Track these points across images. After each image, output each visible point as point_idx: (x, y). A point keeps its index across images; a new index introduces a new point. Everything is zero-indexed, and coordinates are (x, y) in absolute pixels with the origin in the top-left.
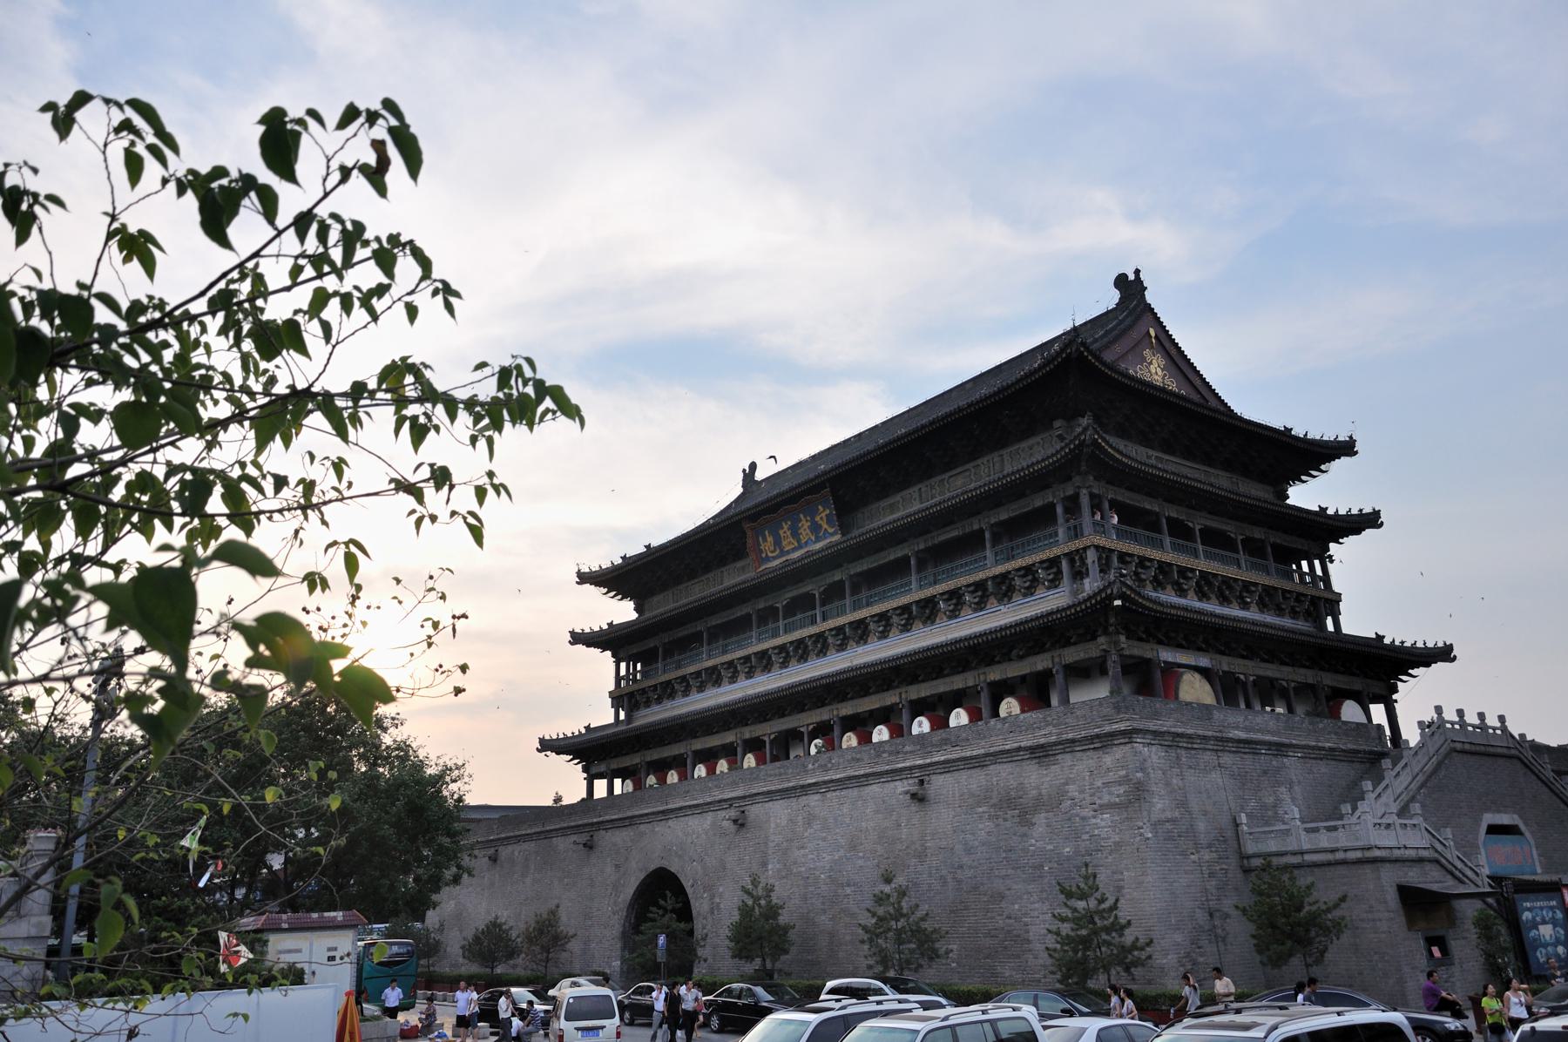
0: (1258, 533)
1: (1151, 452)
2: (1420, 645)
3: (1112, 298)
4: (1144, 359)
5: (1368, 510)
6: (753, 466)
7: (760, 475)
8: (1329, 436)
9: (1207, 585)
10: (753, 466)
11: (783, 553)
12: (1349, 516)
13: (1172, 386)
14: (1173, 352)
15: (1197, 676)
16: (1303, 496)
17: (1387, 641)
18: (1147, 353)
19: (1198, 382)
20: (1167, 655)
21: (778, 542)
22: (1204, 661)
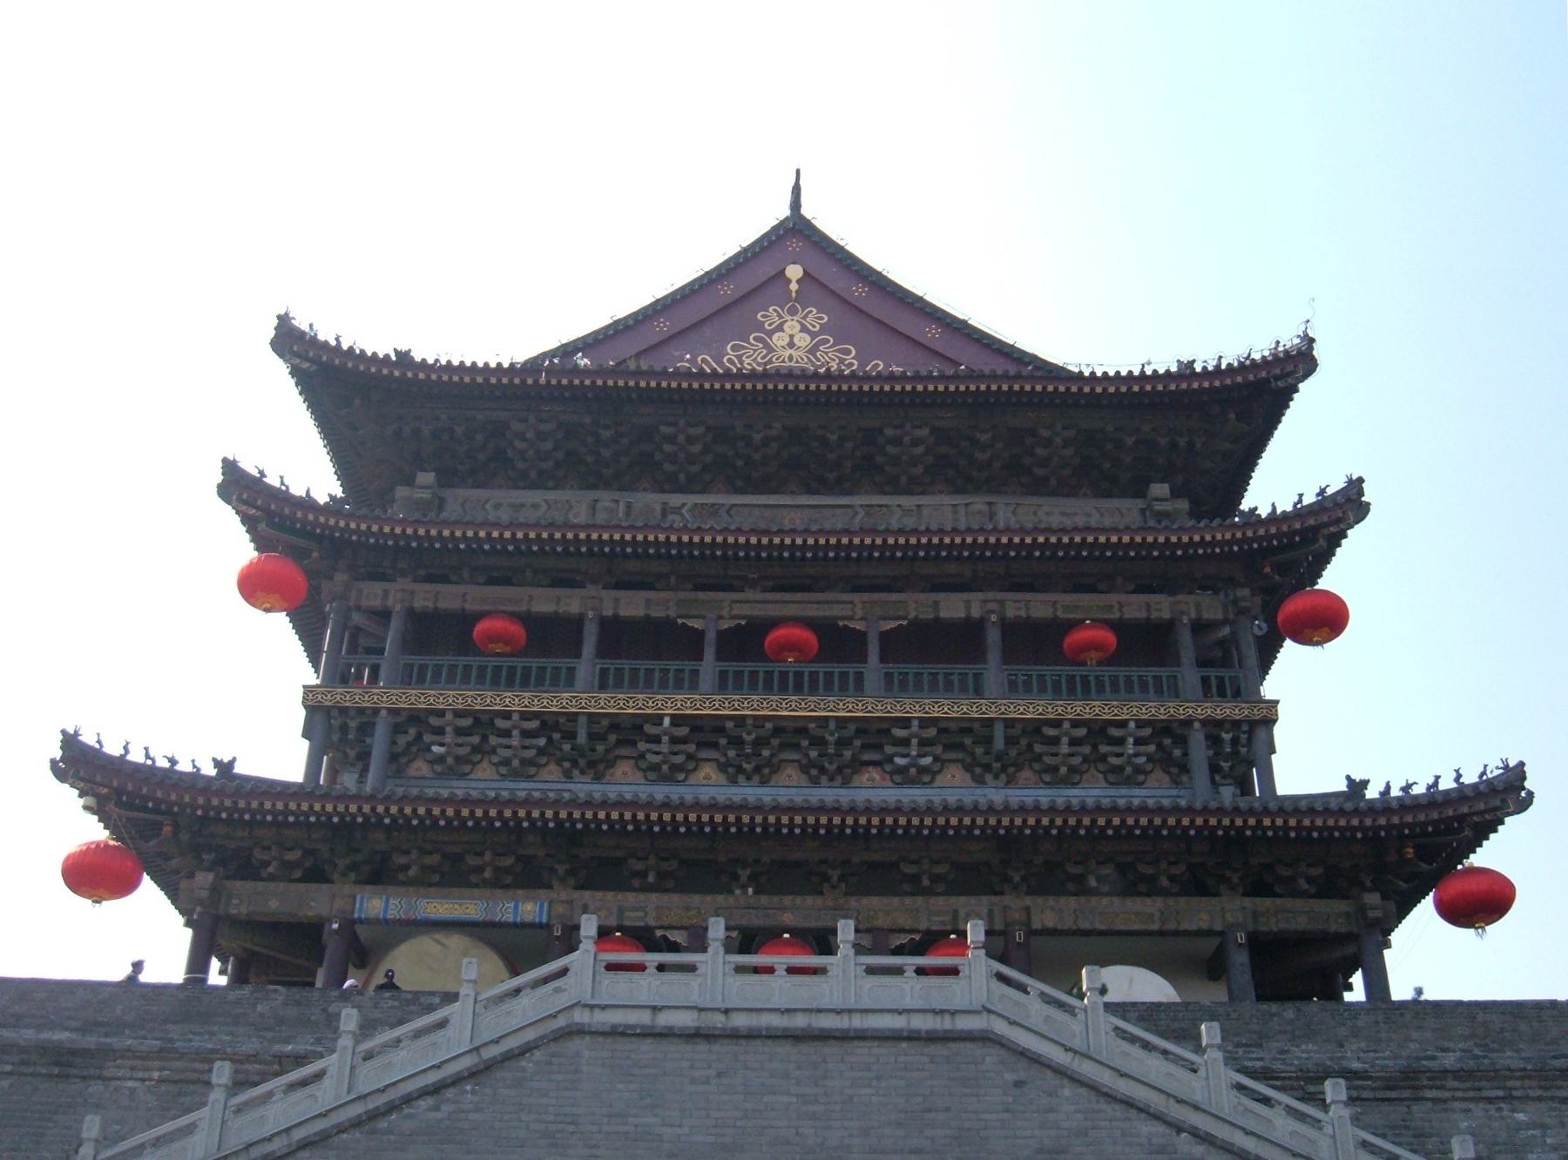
0: (953, 607)
1: (676, 499)
2: (1447, 784)
4: (760, 327)
5: (1336, 485)
8: (1260, 349)
13: (840, 359)
14: (858, 292)
15: (456, 941)
18: (771, 315)
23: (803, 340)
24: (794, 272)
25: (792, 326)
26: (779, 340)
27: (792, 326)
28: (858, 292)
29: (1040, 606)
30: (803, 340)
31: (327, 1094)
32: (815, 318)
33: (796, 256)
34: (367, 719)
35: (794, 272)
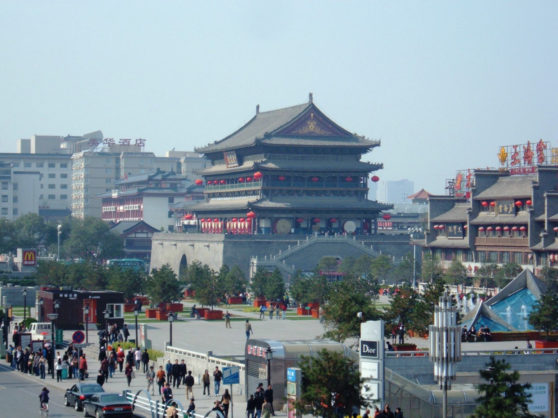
1: (299, 155)
3: (306, 100)
4: (307, 124)
6: (258, 107)
7: (261, 110)
8: (374, 140)
9: (309, 193)
10: (258, 107)
11: (231, 164)
12: (375, 165)
15: (285, 220)
16: (365, 158)
17: (378, 202)
18: (309, 122)
19: (330, 126)
20: (276, 215)
21: (230, 160)
22: (291, 216)
23: (313, 127)
24: (312, 115)
25: (312, 125)
26: (310, 127)
27: (312, 125)
28: (321, 118)
29: (343, 175)
30: (313, 127)
31: (298, 248)
32: (315, 123)
33: (312, 112)
34: (268, 190)
35: (312, 115)
